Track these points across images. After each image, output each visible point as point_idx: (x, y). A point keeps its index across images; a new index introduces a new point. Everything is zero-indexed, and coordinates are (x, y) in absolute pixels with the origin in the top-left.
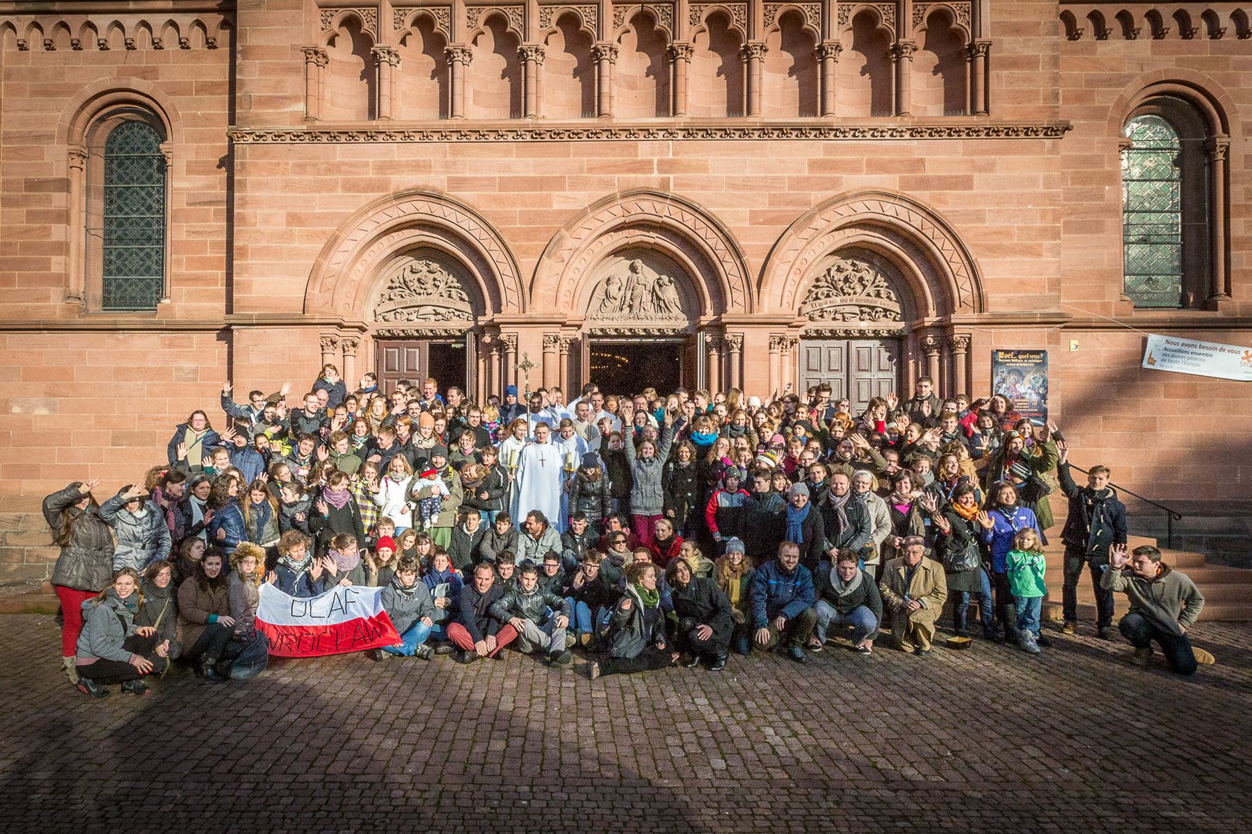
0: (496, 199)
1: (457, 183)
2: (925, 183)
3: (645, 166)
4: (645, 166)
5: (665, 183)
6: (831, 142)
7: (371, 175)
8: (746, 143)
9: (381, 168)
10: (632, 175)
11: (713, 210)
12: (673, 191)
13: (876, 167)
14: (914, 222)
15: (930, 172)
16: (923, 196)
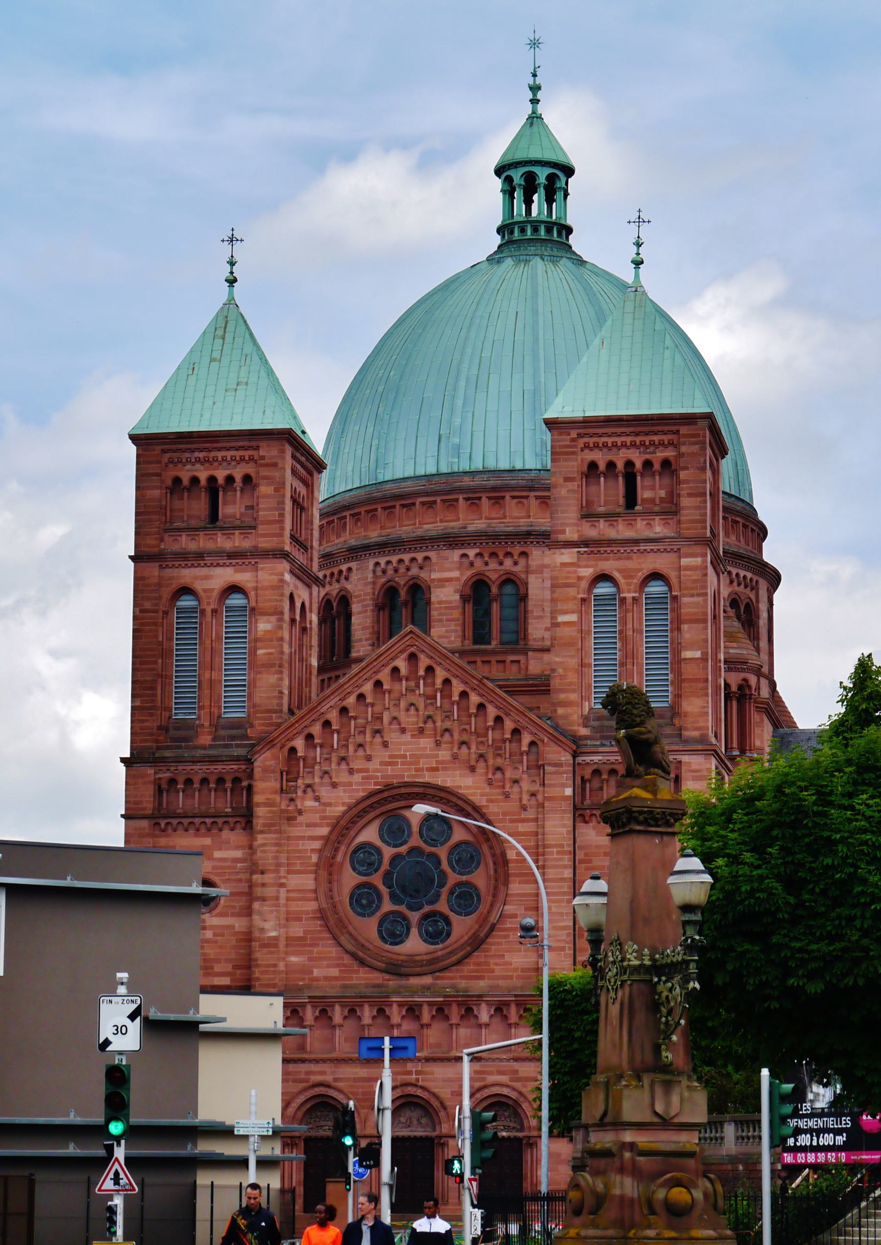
0: (352, 1086)
1: (336, 1080)
2: (518, 1080)
3: (410, 1073)
4: (410, 1073)
5: (417, 1080)
6: (483, 1063)
7: (303, 1076)
8: (449, 1063)
9: (308, 1073)
10: (405, 1077)
11: (436, 1090)
12: (420, 1083)
13: (501, 1073)
14: (514, 1095)
15: (521, 1075)
16: (517, 1085)
